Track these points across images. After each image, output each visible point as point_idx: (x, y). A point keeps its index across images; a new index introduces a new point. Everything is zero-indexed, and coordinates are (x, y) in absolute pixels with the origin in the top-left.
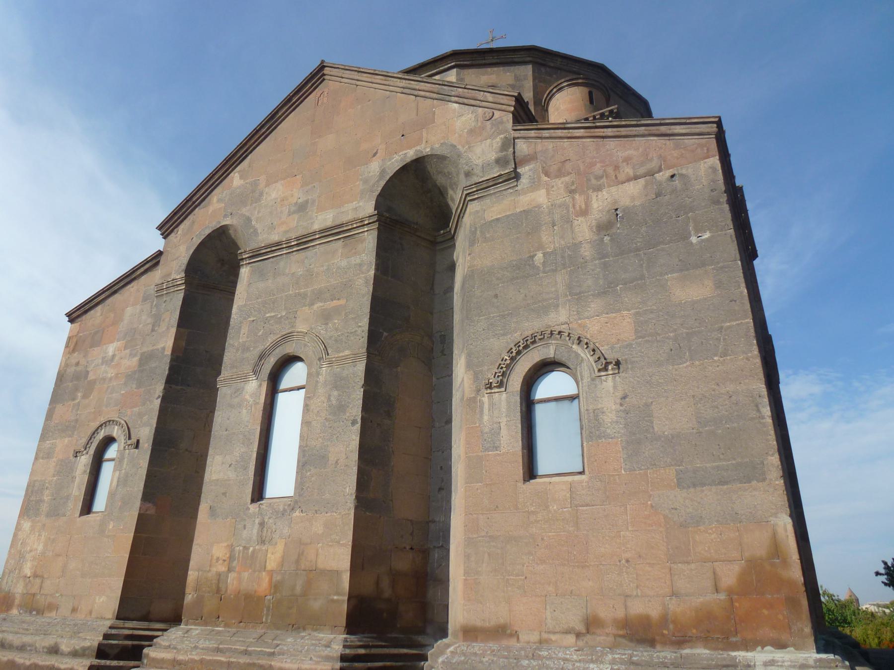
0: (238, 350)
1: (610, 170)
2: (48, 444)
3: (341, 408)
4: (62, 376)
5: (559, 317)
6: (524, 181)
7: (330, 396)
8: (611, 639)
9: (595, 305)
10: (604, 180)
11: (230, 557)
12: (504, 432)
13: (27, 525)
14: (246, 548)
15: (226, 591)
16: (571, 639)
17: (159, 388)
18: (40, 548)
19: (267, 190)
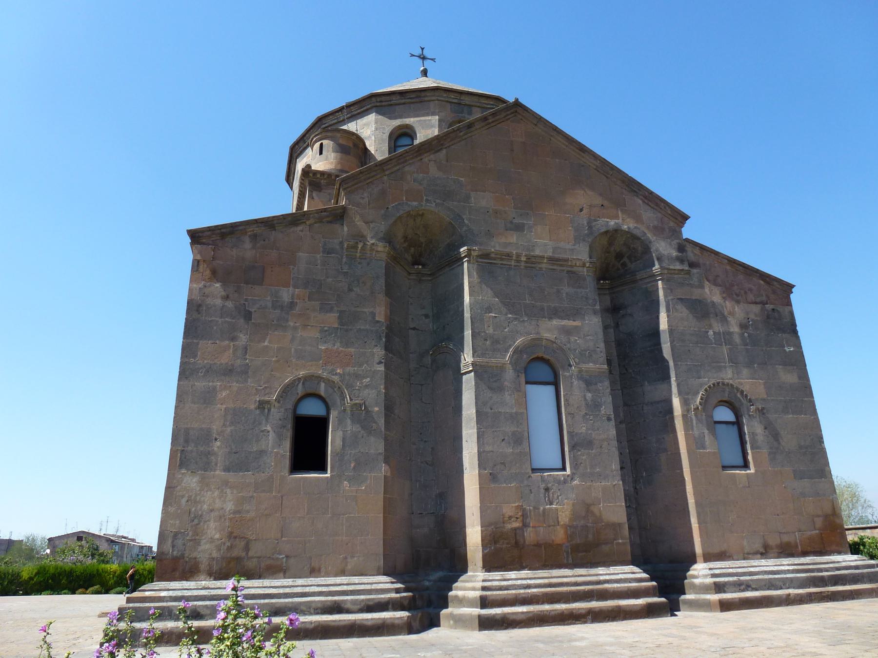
0: (486, 340)
1: (742, 292)
2: (200, 384)
3: (595, 406)
4: (200, 306)
5: (728, 375)
6: (695, 281)
7: (585, 396)
8: (776, 555)
9: (745, 372)
10: (740, 298)
11: (523, 515)
12: (707, 438)
13: (191, 481)
14: (536, 508)
15: (524, 542)
16: (759, 556)
17: (379, 352)
18: (230, 506)
19: (473, 194)
